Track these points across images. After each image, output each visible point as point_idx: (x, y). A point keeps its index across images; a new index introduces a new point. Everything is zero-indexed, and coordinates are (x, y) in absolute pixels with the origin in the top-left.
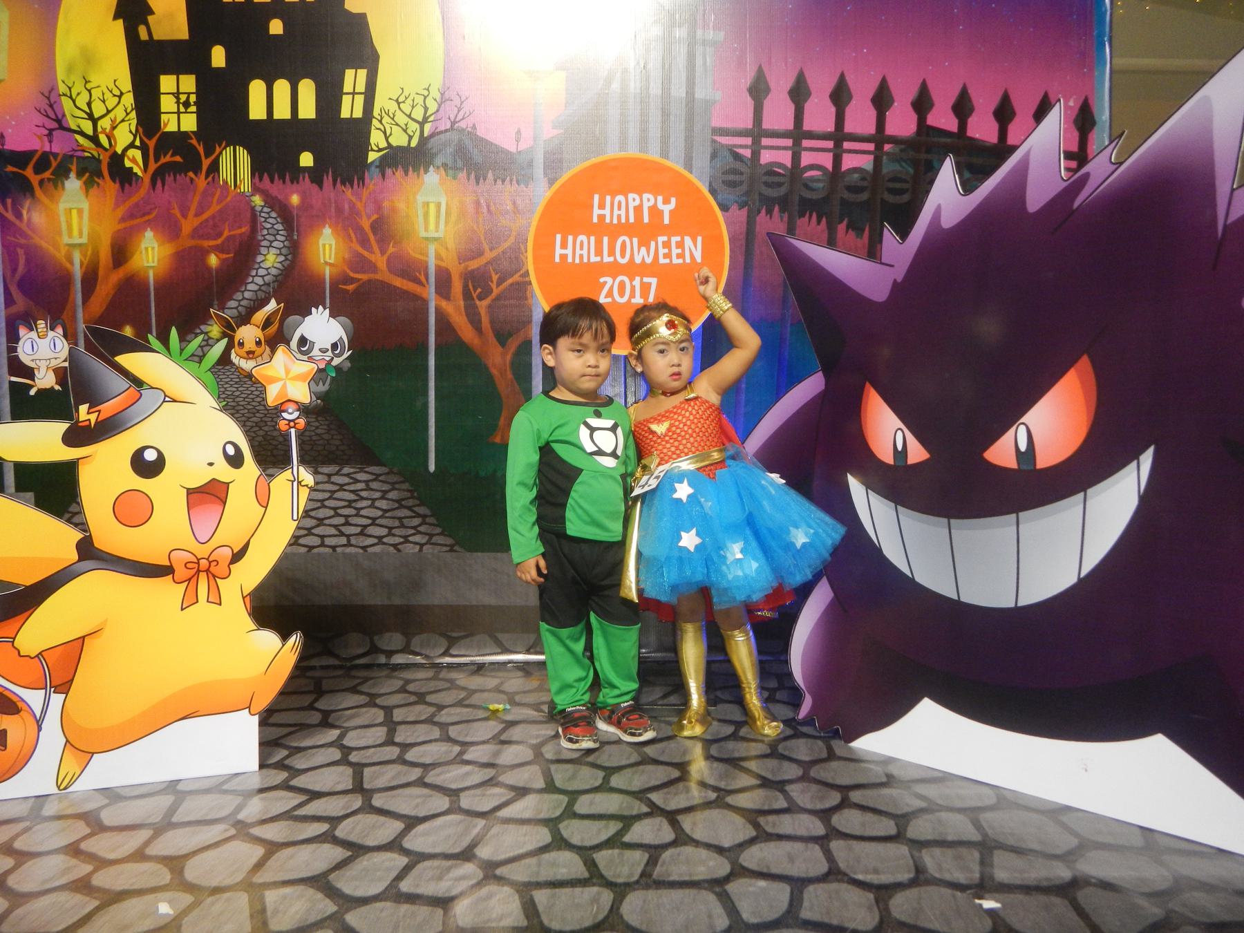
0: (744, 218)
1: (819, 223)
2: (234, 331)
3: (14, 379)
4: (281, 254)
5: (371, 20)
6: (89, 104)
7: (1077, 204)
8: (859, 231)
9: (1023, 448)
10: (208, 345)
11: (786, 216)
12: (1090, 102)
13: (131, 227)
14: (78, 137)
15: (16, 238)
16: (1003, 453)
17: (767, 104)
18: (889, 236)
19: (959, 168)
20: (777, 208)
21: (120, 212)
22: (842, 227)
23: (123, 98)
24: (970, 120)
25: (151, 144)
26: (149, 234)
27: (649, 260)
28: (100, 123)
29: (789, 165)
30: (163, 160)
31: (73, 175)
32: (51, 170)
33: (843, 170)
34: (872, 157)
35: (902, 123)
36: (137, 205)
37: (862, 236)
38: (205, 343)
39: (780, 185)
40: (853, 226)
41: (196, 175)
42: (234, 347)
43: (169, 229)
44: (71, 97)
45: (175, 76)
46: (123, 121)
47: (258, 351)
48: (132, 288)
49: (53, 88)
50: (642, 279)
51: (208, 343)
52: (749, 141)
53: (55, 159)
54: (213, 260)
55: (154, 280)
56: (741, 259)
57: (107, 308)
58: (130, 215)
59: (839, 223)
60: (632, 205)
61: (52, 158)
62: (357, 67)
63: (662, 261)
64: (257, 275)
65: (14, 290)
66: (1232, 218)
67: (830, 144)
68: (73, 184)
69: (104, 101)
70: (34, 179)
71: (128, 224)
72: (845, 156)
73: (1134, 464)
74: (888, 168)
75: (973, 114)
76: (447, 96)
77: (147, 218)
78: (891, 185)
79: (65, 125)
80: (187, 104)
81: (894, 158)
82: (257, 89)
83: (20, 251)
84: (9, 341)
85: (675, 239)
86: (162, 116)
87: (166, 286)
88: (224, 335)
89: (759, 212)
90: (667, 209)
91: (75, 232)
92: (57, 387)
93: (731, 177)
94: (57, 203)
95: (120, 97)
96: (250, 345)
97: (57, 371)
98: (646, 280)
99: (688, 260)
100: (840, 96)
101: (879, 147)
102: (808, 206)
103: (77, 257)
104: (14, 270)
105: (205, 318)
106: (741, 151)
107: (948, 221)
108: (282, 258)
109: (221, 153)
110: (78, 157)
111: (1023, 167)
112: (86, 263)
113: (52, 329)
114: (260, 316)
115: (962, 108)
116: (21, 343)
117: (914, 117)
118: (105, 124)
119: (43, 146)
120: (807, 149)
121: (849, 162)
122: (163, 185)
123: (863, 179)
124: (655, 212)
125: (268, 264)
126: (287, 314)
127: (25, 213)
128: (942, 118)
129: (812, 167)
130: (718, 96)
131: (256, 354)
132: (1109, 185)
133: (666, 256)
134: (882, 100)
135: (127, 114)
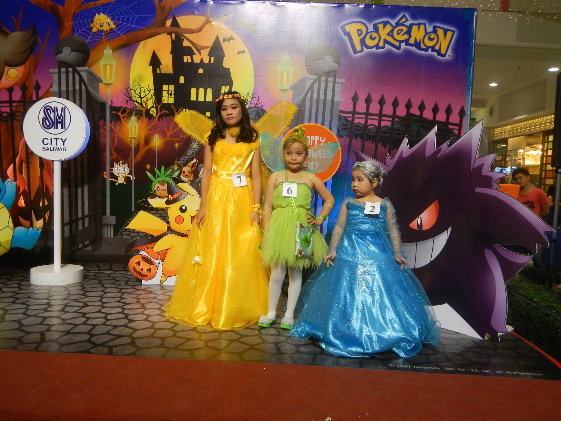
0: (348, 141)
1: (372, 143)
2: (182, 168)
3: (111, 179)
4: (198, 144)
5: (231, 70)
6: (140, 93)
7: (438, 156)
8: (385, 146)
9: (419, 224)
10: (173, 172)
11: (362, 141)
12: (464, 107)
13: (151, 133)
14: (136, 103)
15: (114, 134)
16: (414, 225)
17: (358, 104)
18: (388, 157)
19: (409, 140)
20: (359, 138)
21: (148, 128)
22: (380, 145)
23: (151, 91)
24: (424, 112)
25: (159, 107)
26: (157, 136)
27: (316, 157)
28: (143, 99)
29: (364, 124)
30: (162, 112)
31: (133, 115)
32: (126, 113)
33: (381, 126)
34: (391, 122)
35: (401, 111)
36: (154, 126)
37: (386, 148)
38: (172, 171)
39: (360, 130)
40: (384, 145)
41: (173, 117)
42: (182, 173)
43: (163, 134)
44: (134, 90)
45: (167, 86)
46: (150, 99)
47: (189, 175)
48: (151, 152)
49: (129, 87)
50: (314, 163)
51: (174, 172)
52: (351, 115)
53: (128, 110)
54: (177, 145)
55: (158, 151)
56: (346, 153)
57: (142, 158)
58: (151, 129)
59: (379, 143)
60: (312, 139)
61: (127, 109)
62: (226, 85)
63: (320, 157)
64: (190, 151)
65: (113, 151)
66: (474, 167)
67: (377, 118)
68: (133, 118)
69: (145, 92)
70: (121, 116)
71: (150, 132)
72: (382, 121)
73: (446, 231)
74: (396, 126)
75: (425, 110)
76: (254, 96)
77: (156, 130)
78: (397, 132)
79: (132, 99)
80: (171, 94)
81: (398, 123)
82: (193, 91)
83: (116, 139)
84: (110, 167)
85: (325, 151)
86: (163, 98)
87: (160, 152)
88: (179, 169)
89: (353, 138)
90: (323, 141)
91: (133, 134)
92: (125, 183)
93: (345, 127)
94: (128, 124)
95: (150, 91)
96: (187, 173)
97: (125, 178)
98: (315, 163)
99: (328, 157)
100: (382, 102)
101: (393, 119)
102: (369, 137)
103: (133, 142)
104: (113, 145)
105: (173, 163)
106: (348, 118)
107: (405, 155)
108: (198, 146)
109: (181, 111)
110: (136, 110)
111: (425, 143)
112: (136, 143)
113: (124, 164)
114: (190, 164)
115: (422, 107)
116: (114, 168)
117: (405, 110)
118: (144, 99)
119: (125, 105)
120: (369, 119)
121: (383, 124)
122: (162, 120)
123: (388, 129)
124: (319, 142)
125: (194, 147)
126: (199, 163)
127: (117, 126)
128: (415, 111)
129: (371, 125)
130: (342, 100)
131: (189, 176)
132: (447, 152)
133: (322, 156)
134: (395, 104)
135: (152, 97)
